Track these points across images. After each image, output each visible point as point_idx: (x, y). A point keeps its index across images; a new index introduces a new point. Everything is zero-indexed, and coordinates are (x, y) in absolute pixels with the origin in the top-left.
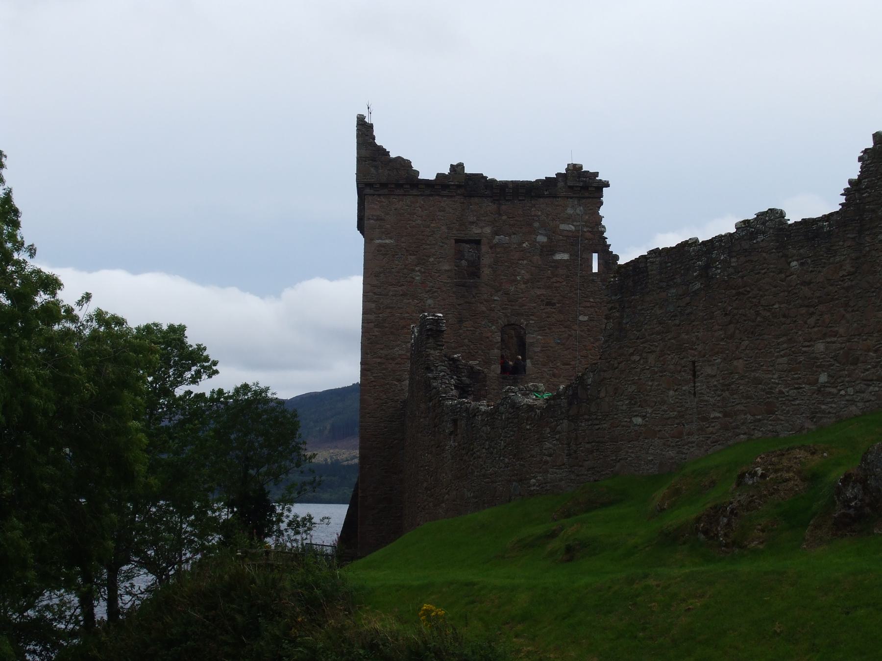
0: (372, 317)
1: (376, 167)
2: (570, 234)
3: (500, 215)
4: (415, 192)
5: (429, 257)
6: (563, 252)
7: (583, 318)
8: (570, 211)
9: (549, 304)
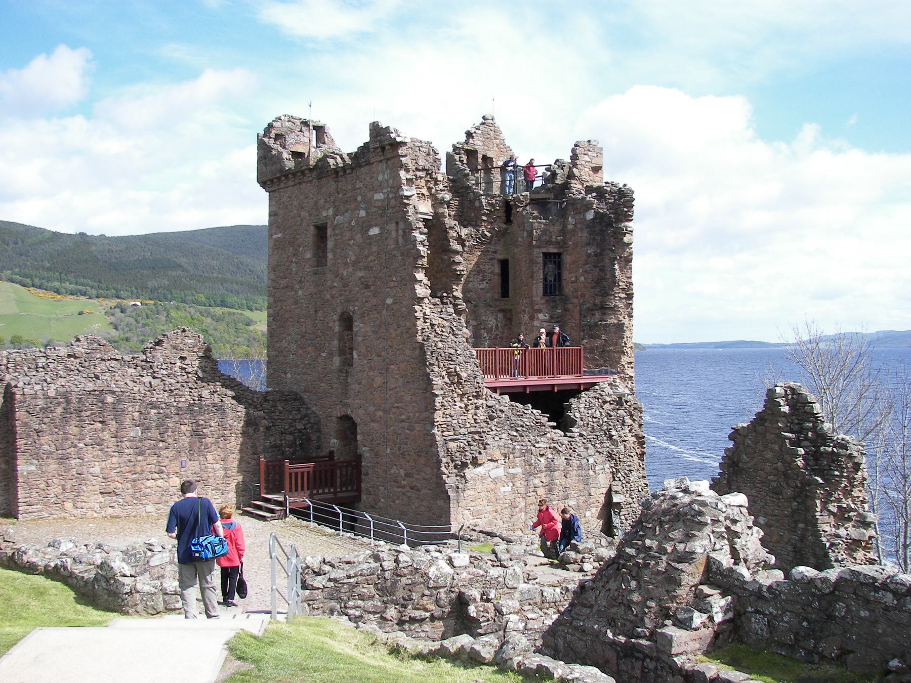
0: (271, 311)
1: (266, 165)
2: (380, 204)
3: (338, 193)
4: (291, 183)
5: (299, 246)
6: (376, 225)
7: (389, 301)
8: (380, 178)
9: (367, 287)
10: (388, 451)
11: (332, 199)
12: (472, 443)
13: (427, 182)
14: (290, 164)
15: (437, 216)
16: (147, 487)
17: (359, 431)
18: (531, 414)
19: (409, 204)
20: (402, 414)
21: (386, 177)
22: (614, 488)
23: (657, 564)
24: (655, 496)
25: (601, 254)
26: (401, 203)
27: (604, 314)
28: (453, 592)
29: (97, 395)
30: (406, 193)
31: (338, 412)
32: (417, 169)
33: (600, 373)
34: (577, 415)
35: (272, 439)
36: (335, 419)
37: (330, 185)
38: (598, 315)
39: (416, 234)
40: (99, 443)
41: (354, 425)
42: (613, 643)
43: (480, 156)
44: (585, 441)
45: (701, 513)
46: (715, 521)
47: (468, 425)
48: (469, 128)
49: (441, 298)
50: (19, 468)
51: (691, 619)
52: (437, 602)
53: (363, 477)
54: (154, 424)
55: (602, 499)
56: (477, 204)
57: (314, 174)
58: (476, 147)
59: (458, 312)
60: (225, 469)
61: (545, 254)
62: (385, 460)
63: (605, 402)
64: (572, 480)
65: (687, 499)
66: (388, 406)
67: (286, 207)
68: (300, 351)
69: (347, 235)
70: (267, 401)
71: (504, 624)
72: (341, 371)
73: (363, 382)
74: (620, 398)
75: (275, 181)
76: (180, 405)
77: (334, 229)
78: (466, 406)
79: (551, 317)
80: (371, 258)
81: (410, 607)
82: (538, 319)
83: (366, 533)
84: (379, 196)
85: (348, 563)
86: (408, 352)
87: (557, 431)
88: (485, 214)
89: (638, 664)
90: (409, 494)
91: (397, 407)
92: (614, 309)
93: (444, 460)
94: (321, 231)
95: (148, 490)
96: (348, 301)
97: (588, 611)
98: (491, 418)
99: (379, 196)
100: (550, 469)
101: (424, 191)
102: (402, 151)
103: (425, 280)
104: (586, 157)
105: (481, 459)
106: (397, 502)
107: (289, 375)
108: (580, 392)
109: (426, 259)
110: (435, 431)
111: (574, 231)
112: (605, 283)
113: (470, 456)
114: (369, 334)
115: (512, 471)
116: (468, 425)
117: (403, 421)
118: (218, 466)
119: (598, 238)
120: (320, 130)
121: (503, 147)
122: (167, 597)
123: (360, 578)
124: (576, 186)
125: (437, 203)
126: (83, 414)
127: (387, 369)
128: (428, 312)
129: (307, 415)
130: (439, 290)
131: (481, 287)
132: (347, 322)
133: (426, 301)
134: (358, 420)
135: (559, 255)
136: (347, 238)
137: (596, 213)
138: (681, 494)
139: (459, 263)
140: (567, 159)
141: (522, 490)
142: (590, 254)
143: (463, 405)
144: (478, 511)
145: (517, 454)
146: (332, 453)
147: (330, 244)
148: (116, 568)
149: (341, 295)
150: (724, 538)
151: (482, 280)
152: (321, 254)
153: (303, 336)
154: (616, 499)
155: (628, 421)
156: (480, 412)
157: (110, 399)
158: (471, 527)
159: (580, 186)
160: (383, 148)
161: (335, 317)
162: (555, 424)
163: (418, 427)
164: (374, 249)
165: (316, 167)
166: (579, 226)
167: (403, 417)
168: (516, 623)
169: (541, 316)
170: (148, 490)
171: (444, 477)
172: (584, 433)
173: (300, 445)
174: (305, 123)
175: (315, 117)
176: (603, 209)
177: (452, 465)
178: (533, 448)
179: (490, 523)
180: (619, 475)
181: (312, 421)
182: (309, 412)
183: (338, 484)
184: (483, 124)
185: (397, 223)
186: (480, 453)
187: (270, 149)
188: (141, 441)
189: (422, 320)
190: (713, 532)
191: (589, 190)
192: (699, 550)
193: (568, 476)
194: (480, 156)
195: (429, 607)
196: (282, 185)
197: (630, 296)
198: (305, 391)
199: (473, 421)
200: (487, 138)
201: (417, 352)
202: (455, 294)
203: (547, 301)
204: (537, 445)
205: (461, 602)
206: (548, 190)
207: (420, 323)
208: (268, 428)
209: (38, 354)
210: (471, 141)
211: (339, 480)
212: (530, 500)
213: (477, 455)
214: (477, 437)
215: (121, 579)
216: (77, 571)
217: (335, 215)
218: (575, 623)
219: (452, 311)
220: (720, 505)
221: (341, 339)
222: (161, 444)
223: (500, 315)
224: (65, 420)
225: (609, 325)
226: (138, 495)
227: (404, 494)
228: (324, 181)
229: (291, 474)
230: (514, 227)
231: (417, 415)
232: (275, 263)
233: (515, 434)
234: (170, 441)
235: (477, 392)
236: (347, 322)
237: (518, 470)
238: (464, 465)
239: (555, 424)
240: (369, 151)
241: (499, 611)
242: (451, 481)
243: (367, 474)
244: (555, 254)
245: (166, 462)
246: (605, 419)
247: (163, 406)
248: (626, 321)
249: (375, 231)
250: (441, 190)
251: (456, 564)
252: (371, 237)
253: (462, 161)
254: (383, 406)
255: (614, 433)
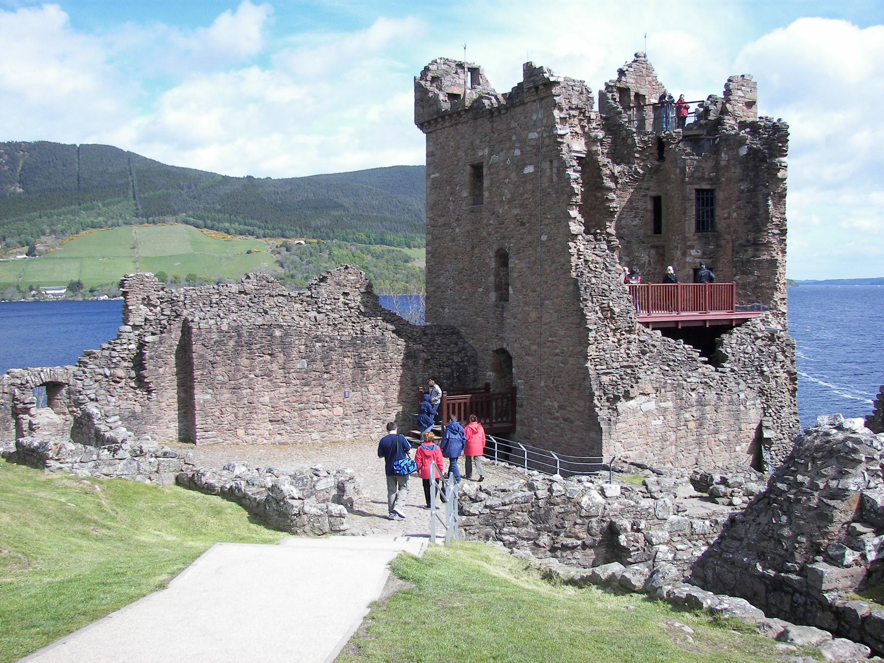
0: (430, 248)
1: (423, 107)
4: (447, 124)
5: (456, 186)
6: (530, 164)
8: (534, 117)
9: (522, 224)
10: (543, 384)
11: (487, 139)
12: (624, 376)
13: (581, 120)
14: (446, 106)
15: (591, 154)
16: (312, 416)
17: (514, 364)
18: (683, 349)
19: (562, 143)
20: (556, 348)
21: (540, 116)
22: (765, 424)
23: (809, 499)
24: (808, 433)
25: (754, 190)
26: (555, 141)
27: (757, 250)
28: (604, 521)
29: (266, 329)
30: (560, 132)
31: (495, 345)
32: (570, 108)
33: (752, 309)
34: (729, 350)
35: (431, 371)
36: (491, 352)
37: (485, 125)
38: (750, 251)
39: (570, 172)
40: (268, 374)
41: (509, 358)
42: (763, 576)
43: (632, 94)
44: (736, 376)
45: (855, 451)
46: (870, 459)
47: (621, 360)
48: (621, 65)
49: (595, 234)
50: (196, 397)
51: (843, 555)
52: (589, 531)
53: (517, 408)
54: (319, 357)
55: (753, 434)
56: (630, 141)
57: (470, 115)
58: (628, 85)
59: (611, 249)
60: (386, 400)
61: (697, 191)
62: (539, 393)
63: (757, 338)
64: (723, 415)
65: (840, 436)
66: (542, 340)
67: (443, 148)
68: (458, 287)
69: (503, 173)
70: (426, 334)
71: (654, 554)
72: (497, 306)
73: (518, 316)
74: (772, 335)
75: (432, 122)
76: (343, 339)
77: (489, 169)
78: (619, 340)
79: (704, 253)
80: (526, 196)
81: (562, 535)
82: (690, 255)
83: (520, 463)
84: (533, 135)
85: (503, 491)
86: (562, 288)
87: (708, 366)
88: (637, 152)
89: (787, 599)
90: (562, 426)
91: (552, 341)
92: (768, 246)
93: (597, 393)
94: (477, 171)
95: (314, 419)
96: (504, 238)
97: (738, 543)
98: (644, 353)
99: (533, 135)
100: (701, 403)
101: (578, 129)
102: (555, 91)
103: (579, 217)
104: (739, 92)
105: (634, 392)
106: (551, 433)
107: (447, 310)
108: (732, 328)
109: (580, 197)
110: (588, 364)
111: (727, 167)
112: (758, 219)
113: (622, 390)
114: (525, 270)
115: (663, 405)
116: (621, 360)
117: (557, 355)
118: (379, 397)
119: (752, 174)
120: (475, 72)
121: (655, 84)
122: (332, 520)
123: (515, 506)
124: (729, 121)
125: (591, 141)
126: (253, 346)
127: (542, 304)
128: (582, 248)
129: (464, 349)
130: (593, 226)
131: (635, 223)
132: (503, 258)
133: (580, 237)
134: (513, 354)
135: (712, 191)
136: (502, 176)
137: (750, 149)
138: (834, 431)
139: (613, 200)
140: (720, 94)
141: (673, 424)
142: (743, 190)
143: (616, 340)
144: (629, 443)
145: (669, 388)
146: (487, 386)
147: (486, 183)
148: (285, 491)
149: (497, 232)
150: (879, 476)
151: (635, 217)
152: (477, 193)
153: (461, 272)
154: (766, 434)
155: (780, 357)
156: (633, 346)
157: (278, 333)
158: (623, 459)
159: (733, 122)
160: (537, 88)
161: (491, 254)
162: (706, 359)
163: (571, 361)
164: (529, 187)
165: (471, 107)
166: (732, 162)
167: (557, 351)
168: (665, 554)
169: (693, 252)
170: (314, 419)
171: (597, 409)
172: (735, 368)
173: (458, 377)
174: (460, 65)
175: (470, 59)
176: (757, 144)
177: (604, 398)
178: (684, 383)
179: (641, 456)
180: (770, 411)
181: (469, 354)
182: (466, 345)
183: (494, 415)
184: (635, 61)
185: (551, 162)
186: (632, 387)
187: (426, 91)
188: (306, 372)
189: (576, 256)
190: (867, 470)
191: (743, 125)
192: (853, 488)
193: (719, 410)
194: (632, 94)
195: (581, 535)
196: (439, 126)
197: (784, 232)
198: (462, 325)
199: (625, 356)
200: (639, 76)
201: (571, 288)
202: (608, 230)
203: (700, 237)
204: (689, 380)
205: (612, 531)
206: (701, 127)
207: (574, 259)
208: (427, 361)
209: (212, 291)
210: (623, 79)
211: (494, 411)
212: (680, 434)
213: (629, 388)
214: (629, 371)
215: (290, 501)
216: (250, 493)
217: (491, 154)
218: (724, 555)
219: (606, 247)
220: (875, 443)
221: (497, 275)
222: (325, 376)
223: (653, 251)
224: (237, 353)
225: (762, 261)
226: (304, 423)
227: (557, 426)
228: (480, 121)
229: (448, 405)
230: (667, 164)
231: (571, 348)
232: (433, 202)
233: (667, 368)
234: (334, 372)
235: (629, 327)
236: (503, 258)
237: (670, 404)
238: (617, 398)
239: (706, 359)
240: (523, 91)
241: (648, 541)
242: (603, 413)
243: (521, 406)
244: (707, 190)
245: (331, 393)
246: (757, 355)
247: (328, 339)
248: (779, 257)
249: (529, 169)
250: (594, 128)
251: (607, 494)
252: (525, 176)
253: (614, 99)
254: (538, 340)
255: (765, 369)
